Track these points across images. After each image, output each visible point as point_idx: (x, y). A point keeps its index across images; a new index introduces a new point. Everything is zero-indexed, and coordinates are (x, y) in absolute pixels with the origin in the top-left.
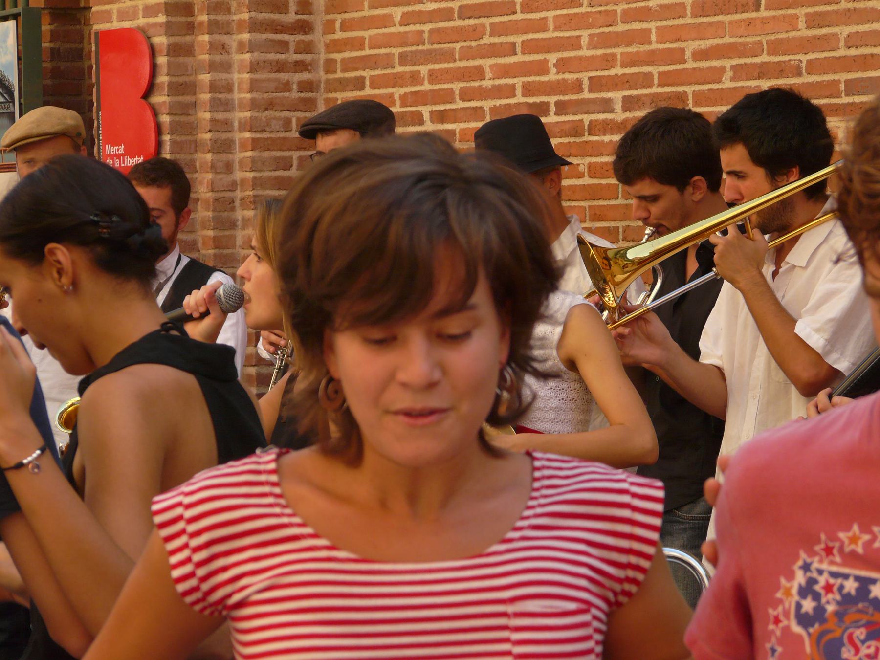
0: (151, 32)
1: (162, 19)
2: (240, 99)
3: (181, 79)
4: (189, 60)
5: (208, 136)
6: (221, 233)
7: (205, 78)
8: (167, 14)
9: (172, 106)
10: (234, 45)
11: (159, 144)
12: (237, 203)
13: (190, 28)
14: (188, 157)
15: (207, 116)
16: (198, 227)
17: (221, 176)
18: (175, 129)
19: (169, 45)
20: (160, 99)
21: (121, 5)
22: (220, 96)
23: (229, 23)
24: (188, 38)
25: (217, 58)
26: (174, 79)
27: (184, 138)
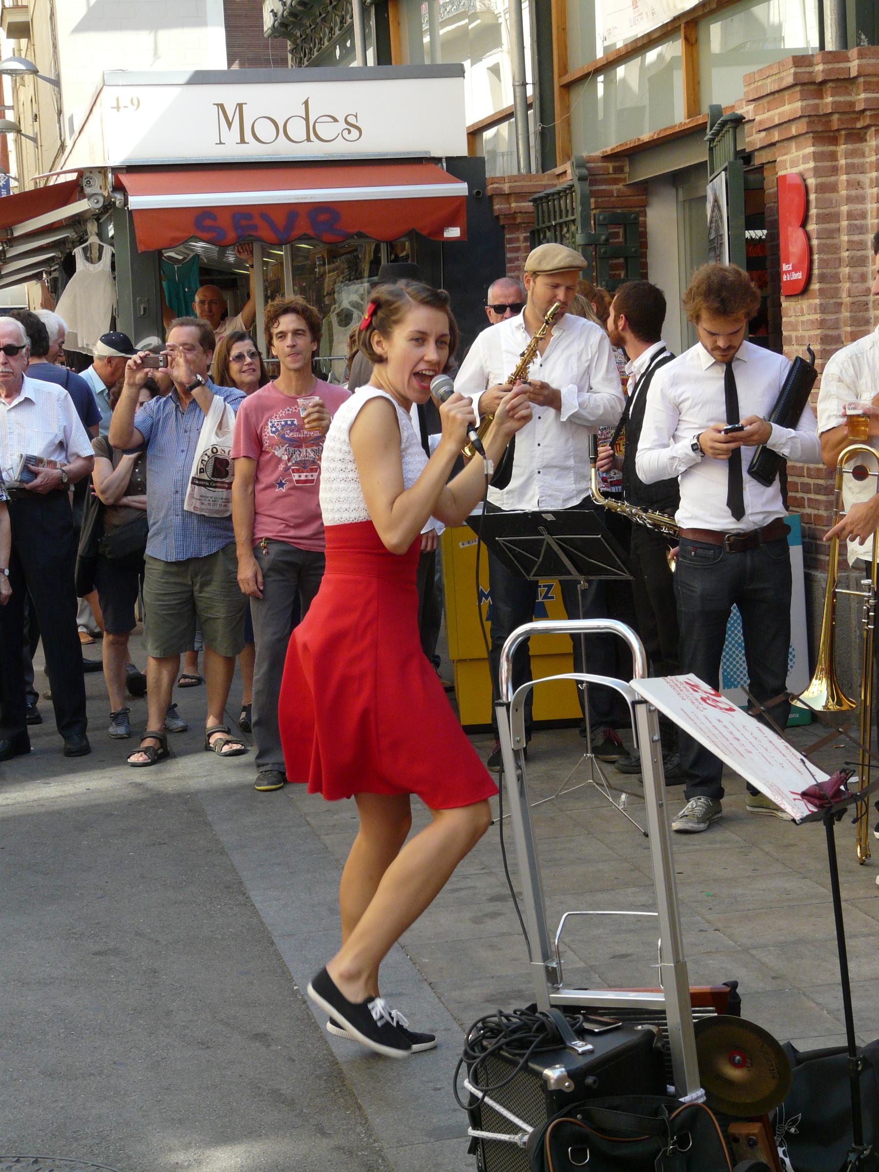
0: (805, 177)
1: (812, 164)
2: (872, 224)
3: (827, 211)
4: (834, 195)
5: (846, 254)
6: (857, 329)
7: (844, 209)
8: (815, 160)
9: (819, 232)
10: (867, 182)
11: (811, 262)
12: (871, 305)
13: (835, 170)
14: (834, 271)
15: (845, 238)
16: (842, 324)
17: (857, 285)
18: (822, 249)
19: (817, 185)
20: (812, 227)
21: (791, 155)
22: (856, 222)
23: (863, 165)
24: (833, 179)
25: (853, 193)
26: (821, 211)
27: (830, 256)
